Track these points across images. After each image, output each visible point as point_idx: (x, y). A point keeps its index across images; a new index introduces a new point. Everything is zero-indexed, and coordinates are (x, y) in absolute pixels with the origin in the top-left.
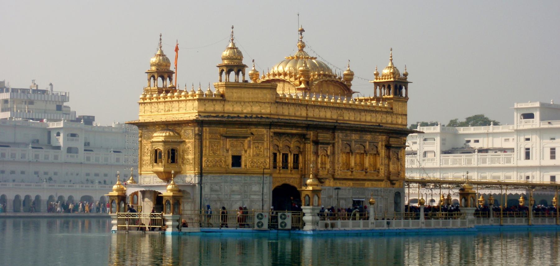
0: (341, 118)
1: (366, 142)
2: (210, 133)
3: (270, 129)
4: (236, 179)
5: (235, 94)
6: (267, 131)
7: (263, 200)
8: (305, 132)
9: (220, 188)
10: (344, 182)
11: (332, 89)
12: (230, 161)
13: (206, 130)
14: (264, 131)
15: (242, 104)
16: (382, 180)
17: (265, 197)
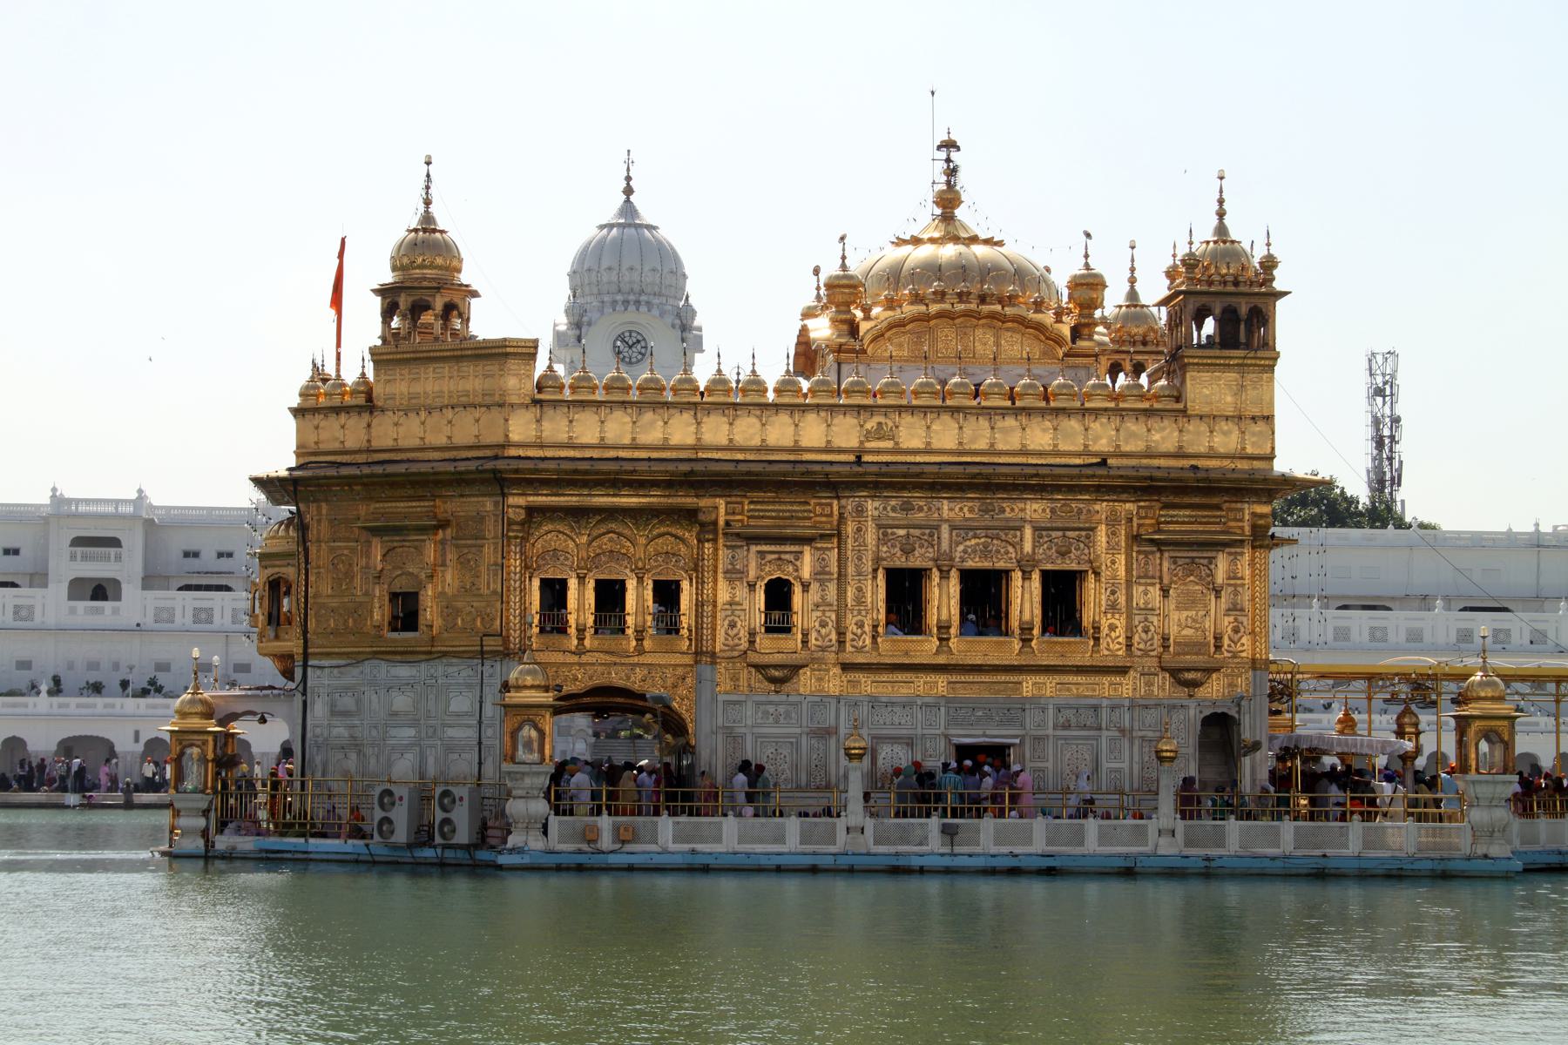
0: (889, 444)
1: (1020, 528)
2: (331, 521)
3: (504, 495)
4: (404, 671)
5: (401, 386)
6: (496, 504)
7: (480, 743)
8: (687, 500)
9: (358, 702)
10: (900, 676)
11: (983, 341)
12: (380, 613)
13: (319, 509)
14: (489, 504)
15: (423, 414)
16: (1122, 671)
17: (489, 732)
